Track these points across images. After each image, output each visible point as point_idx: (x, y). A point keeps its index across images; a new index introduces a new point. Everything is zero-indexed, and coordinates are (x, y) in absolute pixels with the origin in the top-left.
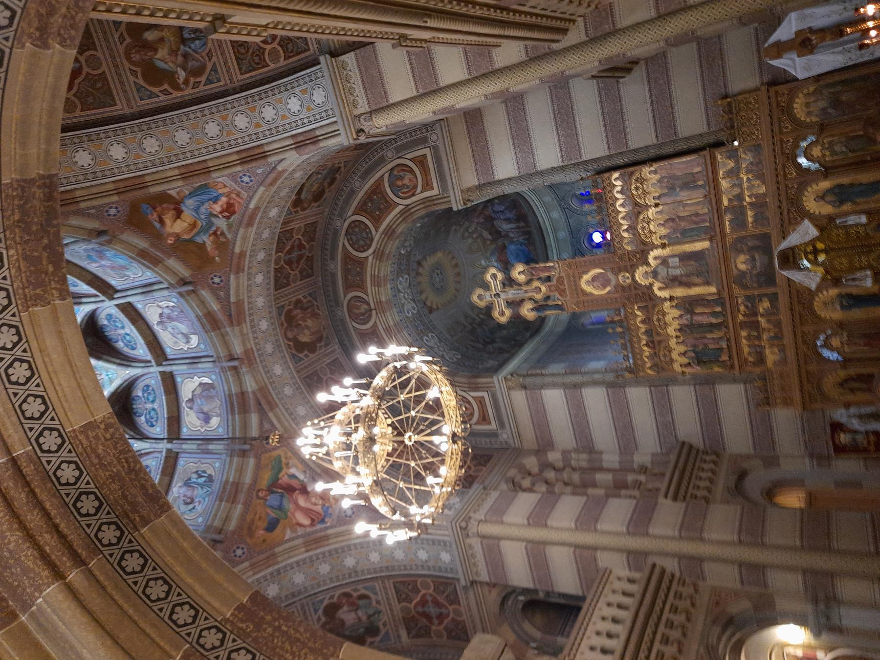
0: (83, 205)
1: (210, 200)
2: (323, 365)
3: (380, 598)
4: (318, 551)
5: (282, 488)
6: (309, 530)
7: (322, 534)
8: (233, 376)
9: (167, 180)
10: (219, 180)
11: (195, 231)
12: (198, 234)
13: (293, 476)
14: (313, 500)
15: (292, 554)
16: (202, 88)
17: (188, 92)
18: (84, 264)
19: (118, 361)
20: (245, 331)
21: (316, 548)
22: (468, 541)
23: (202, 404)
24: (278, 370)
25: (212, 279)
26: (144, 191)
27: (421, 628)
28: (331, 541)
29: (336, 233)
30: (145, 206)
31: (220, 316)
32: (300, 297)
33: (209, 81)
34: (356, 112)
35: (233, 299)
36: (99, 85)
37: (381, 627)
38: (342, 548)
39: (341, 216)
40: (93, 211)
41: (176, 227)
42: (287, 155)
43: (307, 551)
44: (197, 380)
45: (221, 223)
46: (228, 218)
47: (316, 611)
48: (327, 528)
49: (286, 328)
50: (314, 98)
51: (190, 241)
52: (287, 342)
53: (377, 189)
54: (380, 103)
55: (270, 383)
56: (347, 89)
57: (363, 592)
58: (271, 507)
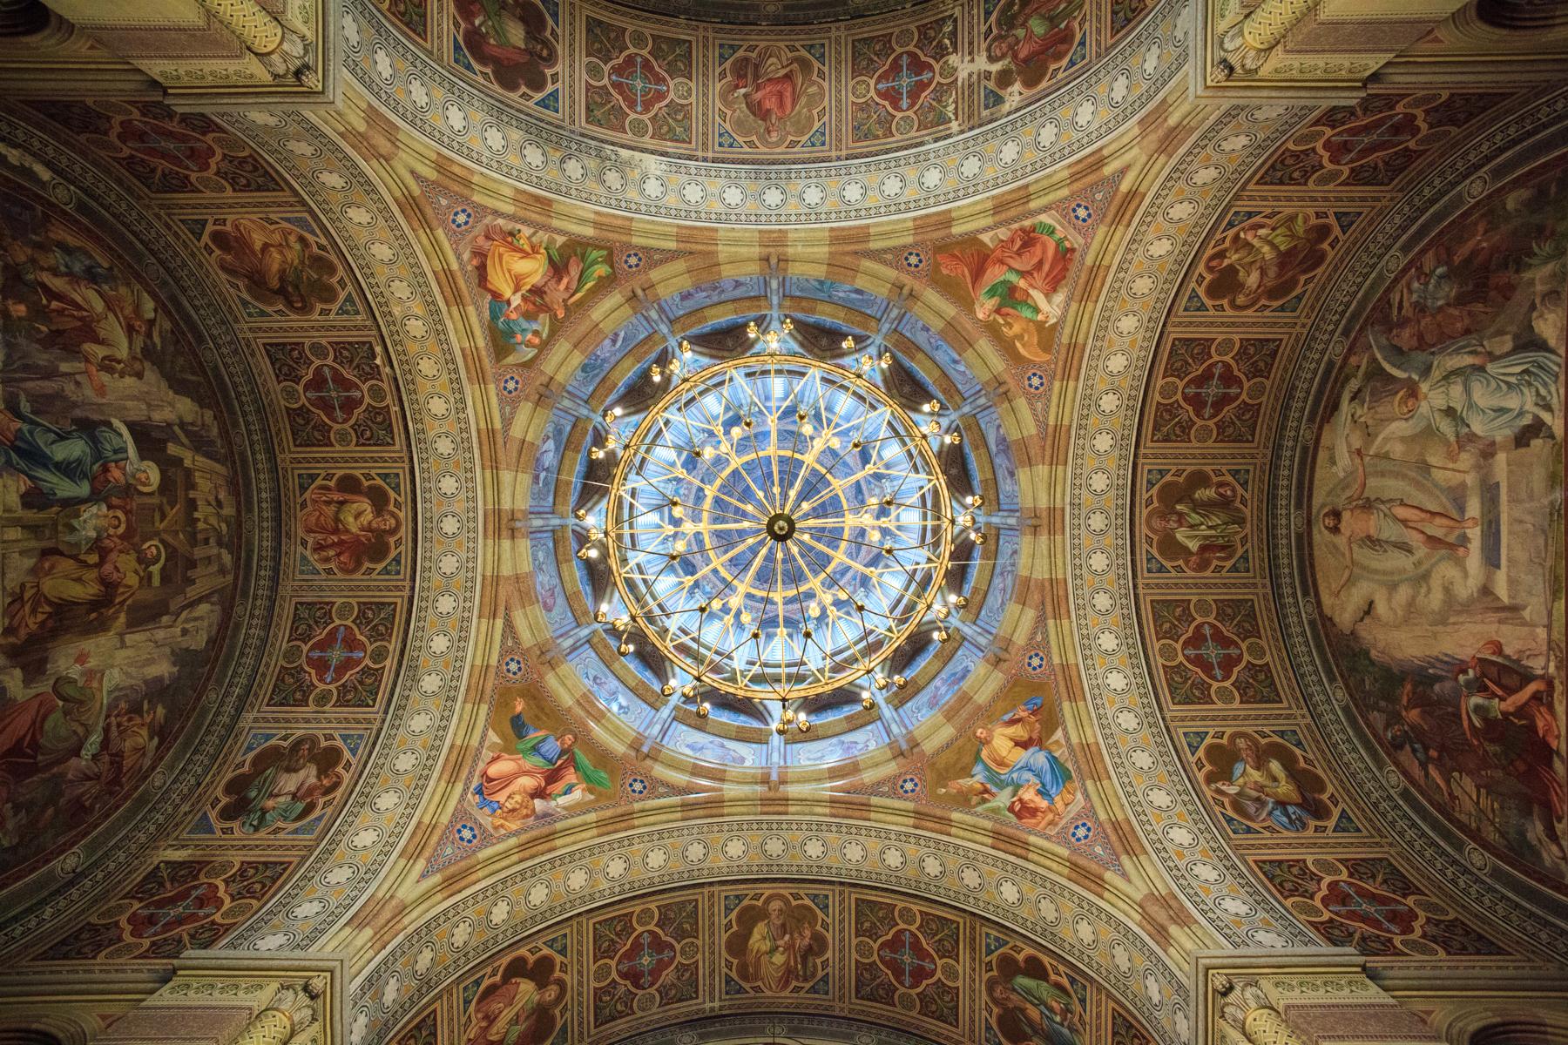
0: (1051, 622)
1: (1044, 786)
2: (699, 956)
3: (281, 835)
4: (440, 762)
5: (560, 768)
6: (481, 766)
7: (463, 776)
9: (1080, 725)
10: (1079, 796)
11: (993, 765)
12: (987, 768)
13: (568, 791)
14: (518, 798)
15: (464, 725)
16: (1217, 809)
17: (1209, 794)
18: (943, 675)
20: (819, 810)
21: (447, 759)
22: (275, 985)
24: (735, 848)
26: (1065, 695)
27: (162, 885)
28: (443, 784)
30: (1039, 701)
32: (829, 954)
33: (1230, 820)
35: (875, 800)
36: (1197, 693)
37: (228, 825)
38: (419, 798)
40: (1039, 638)
41: (1001, 741)
42: (1139, 883)
43: (452, 746)
45: (1003, 799)
46: (1011, 809)
47: (345, 738)
48: (465, 790)
49: (787, 902)
50: (1261, 932)
51: (977, 758)
52: (767, 893)
56: (1308, 978)
57: (317, 813)
58: (543, 740)
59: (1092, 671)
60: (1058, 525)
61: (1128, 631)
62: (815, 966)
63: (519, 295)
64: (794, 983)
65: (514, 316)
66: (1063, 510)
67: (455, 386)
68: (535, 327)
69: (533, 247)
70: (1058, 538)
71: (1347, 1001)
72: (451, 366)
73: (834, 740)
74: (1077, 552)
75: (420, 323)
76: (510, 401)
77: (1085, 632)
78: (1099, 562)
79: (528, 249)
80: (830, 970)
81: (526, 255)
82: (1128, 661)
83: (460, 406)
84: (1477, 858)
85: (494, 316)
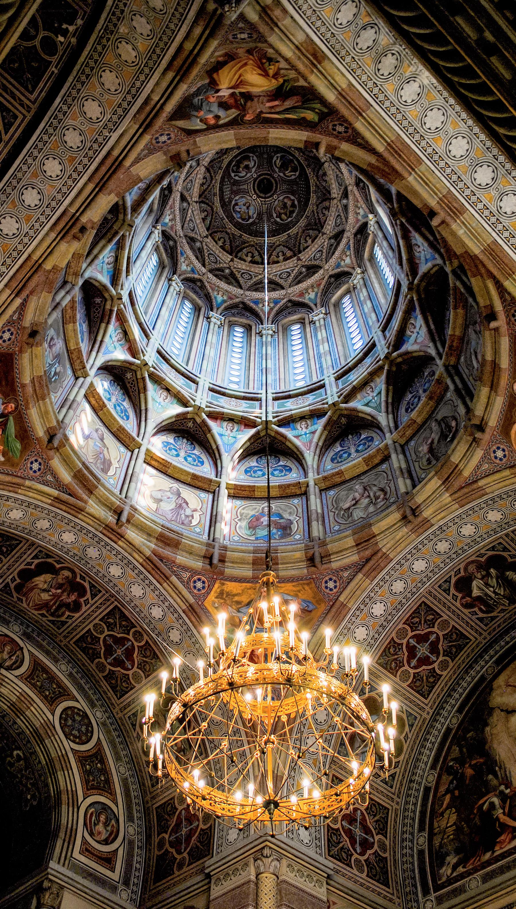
0: (360, 576)
8: (112, 503)
19: (164, 424)
23: (95, 445)
25: (204, 582)
29: (92, 705)
30: (311, 607)
31: (167, 552)
32: (77, 615)
34: (284, 862)
39: (104, 724)
40: (346, 574)
44: (115, 464)
53: (106, 787)
54: (286, 895)
55: (70, 521)
59: (354, 619)
60: (420, 530)
61: (394, 612)
62: (63, 614)
63: (231, 91)
64: (44, 612)
65: (212, 100)
66: (433, 525)
67: (120, 111)
68: (221, 113)
69: (276, 76)
70: (413, 536)
71: (309, 890)
72: (129, 98)
73: (176, 485)
74: (414, 551)
75: (134, 54)
76: (151, 150)
77: (372, 595)
78: (419, 566)
79: (271, 72)
80: (70, 621)
81: (266, 74)
82: (377, 627)
83: (110, 125)
84: (422, 840)
85: (198, 93)
